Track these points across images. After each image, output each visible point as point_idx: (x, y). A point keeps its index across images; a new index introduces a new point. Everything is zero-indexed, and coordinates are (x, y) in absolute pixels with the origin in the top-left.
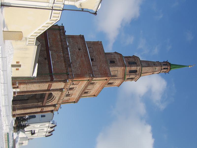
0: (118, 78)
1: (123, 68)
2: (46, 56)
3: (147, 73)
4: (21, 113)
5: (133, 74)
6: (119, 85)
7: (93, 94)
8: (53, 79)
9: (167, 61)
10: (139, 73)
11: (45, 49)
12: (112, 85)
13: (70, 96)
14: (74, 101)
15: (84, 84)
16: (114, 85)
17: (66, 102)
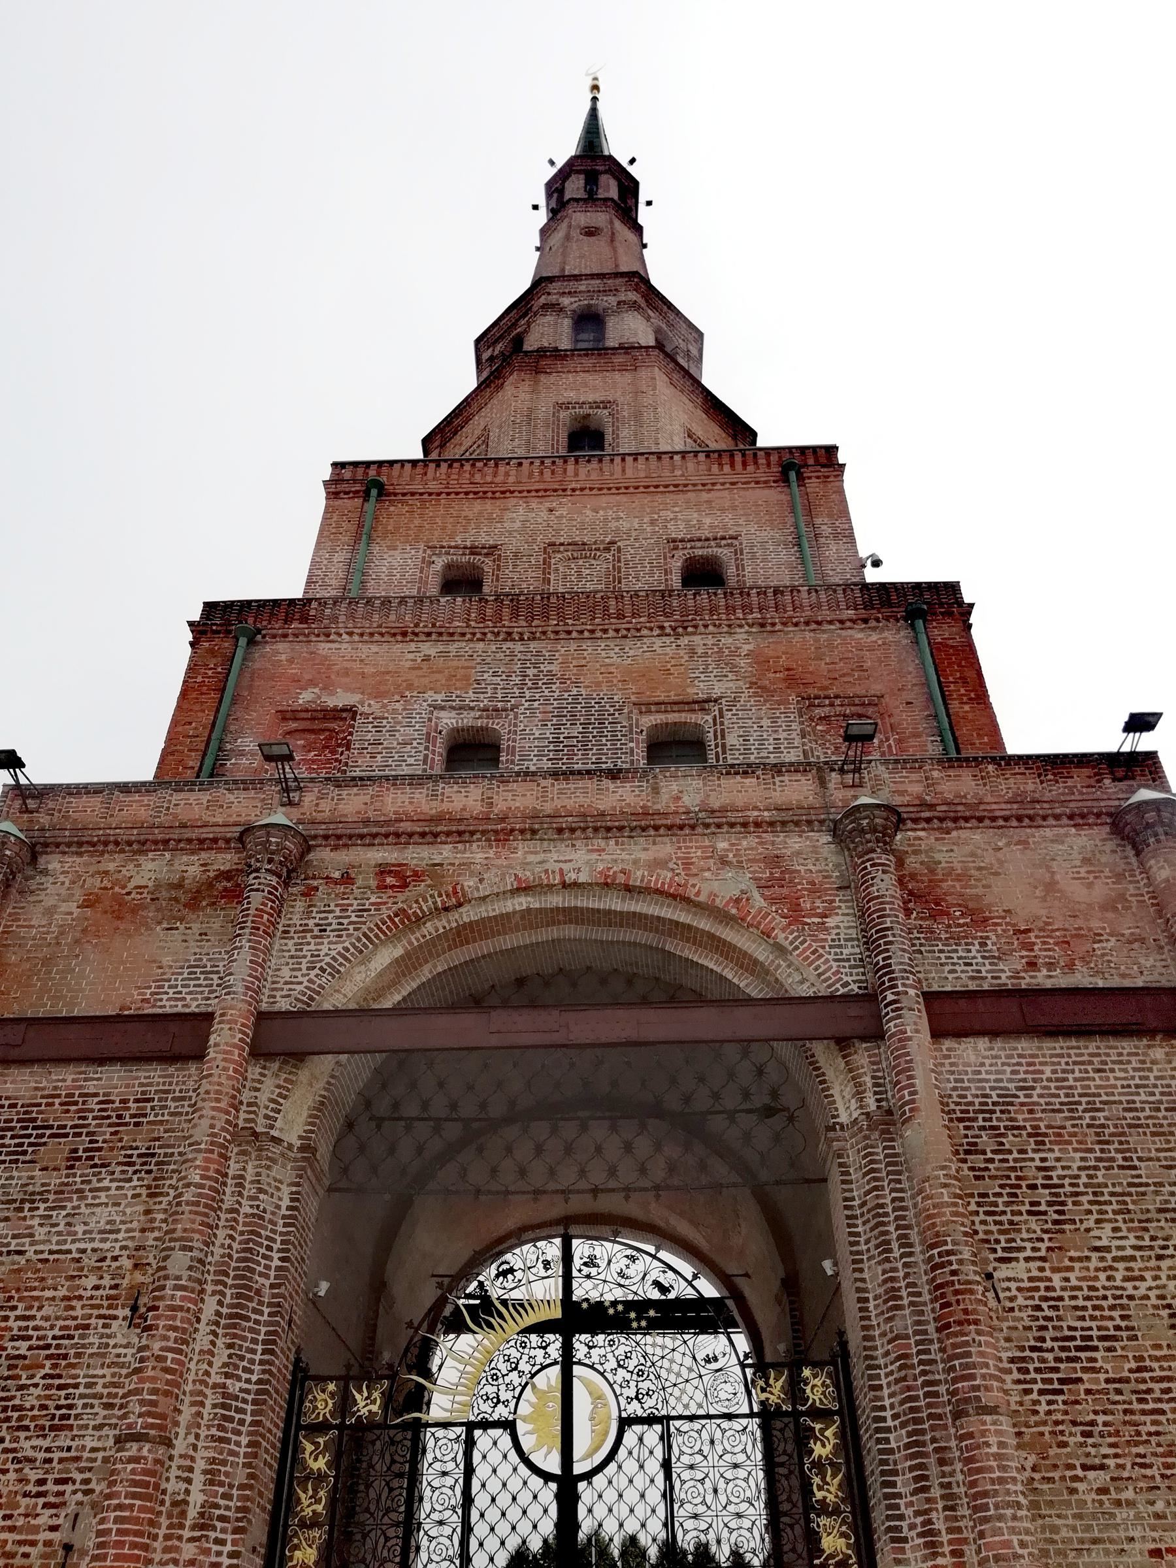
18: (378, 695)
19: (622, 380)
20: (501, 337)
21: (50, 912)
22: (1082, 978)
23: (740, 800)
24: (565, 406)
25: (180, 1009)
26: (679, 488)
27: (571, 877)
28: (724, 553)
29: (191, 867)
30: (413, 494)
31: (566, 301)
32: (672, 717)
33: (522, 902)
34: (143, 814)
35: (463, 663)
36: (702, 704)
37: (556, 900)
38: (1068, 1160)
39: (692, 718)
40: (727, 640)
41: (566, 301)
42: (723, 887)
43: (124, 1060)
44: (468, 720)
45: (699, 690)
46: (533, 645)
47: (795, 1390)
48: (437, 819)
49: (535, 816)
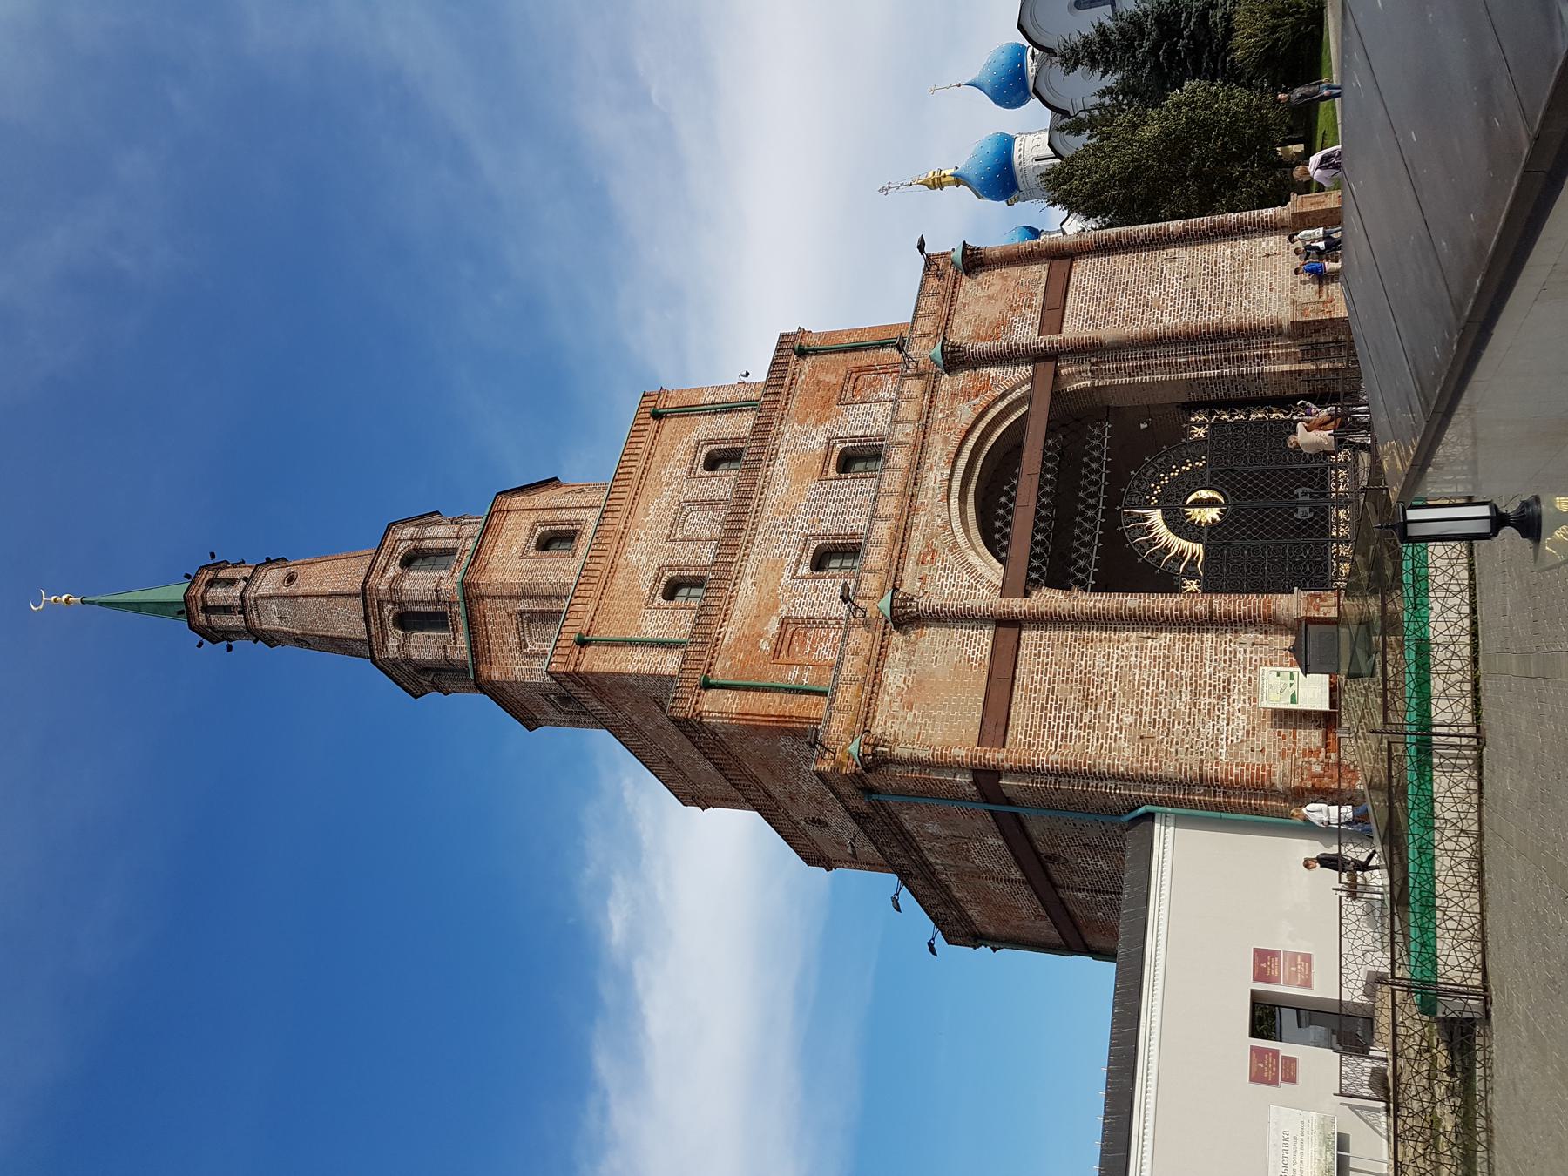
0: (511, 597)
1: (496, 675)
2: (1053, 869)
3: (330, 595)
4: (1245, 244)
5: (417, 608)
6: (495, 520)
7: (669, 425)
8: (975, 782)
9: (230, 648)
10: (381, 610)
11: (1060, 891)
12: (547, 523)
13: (842, 440)
15: (737, 615)
16: (534, 516)
17: (865, 358)
18: (776, 606)
21: (911, 725)
22: (1040, 290)
25: (989, 648)
27: (946, 476)
28: (706, 449)
29: (896, 657)
31: (391, 573)
32: (834, 461)
33: (954, 501)
34: (853, 688)
36: (829, 448)
37: (956, 487)
38: (1121, 302)
41: (391, 573)
42: (966, 414)
43: (1015, 667)
44: (807, 560)
46: (760, 529)
47: (1200, 424)
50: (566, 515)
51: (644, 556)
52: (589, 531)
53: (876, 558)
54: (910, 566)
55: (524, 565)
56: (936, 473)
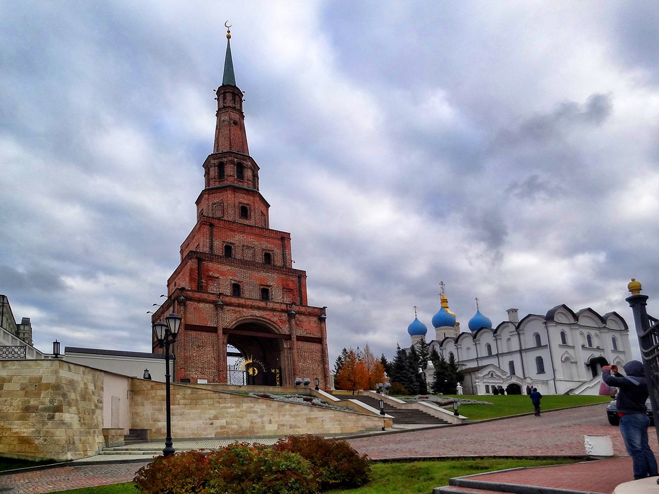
7: (279, 242)
14: (295, 279)
19: (252, 198)
20: (217, 159)
22: (312, 336)
23: (277, 307)
24: (240, 203)
26: (265, 237)
30: (218, 227)
31: (236, 160)
32: (265, 287)
33: (250, 317)
35: (234, 271)
36: (269, 286)
37: (255, 318)
39: (267, 288)
40: (273, 275)
42: (275, 319)
44: (236, 282)
45: (269, 283)
48: (239, 304)
49: (251, 305)
50: (252, 214)
51: (237, 239)
52: (247, 222)
53: (235, 300)
54: (231, 308)
55: (237, 203)
56: (257, 313)
